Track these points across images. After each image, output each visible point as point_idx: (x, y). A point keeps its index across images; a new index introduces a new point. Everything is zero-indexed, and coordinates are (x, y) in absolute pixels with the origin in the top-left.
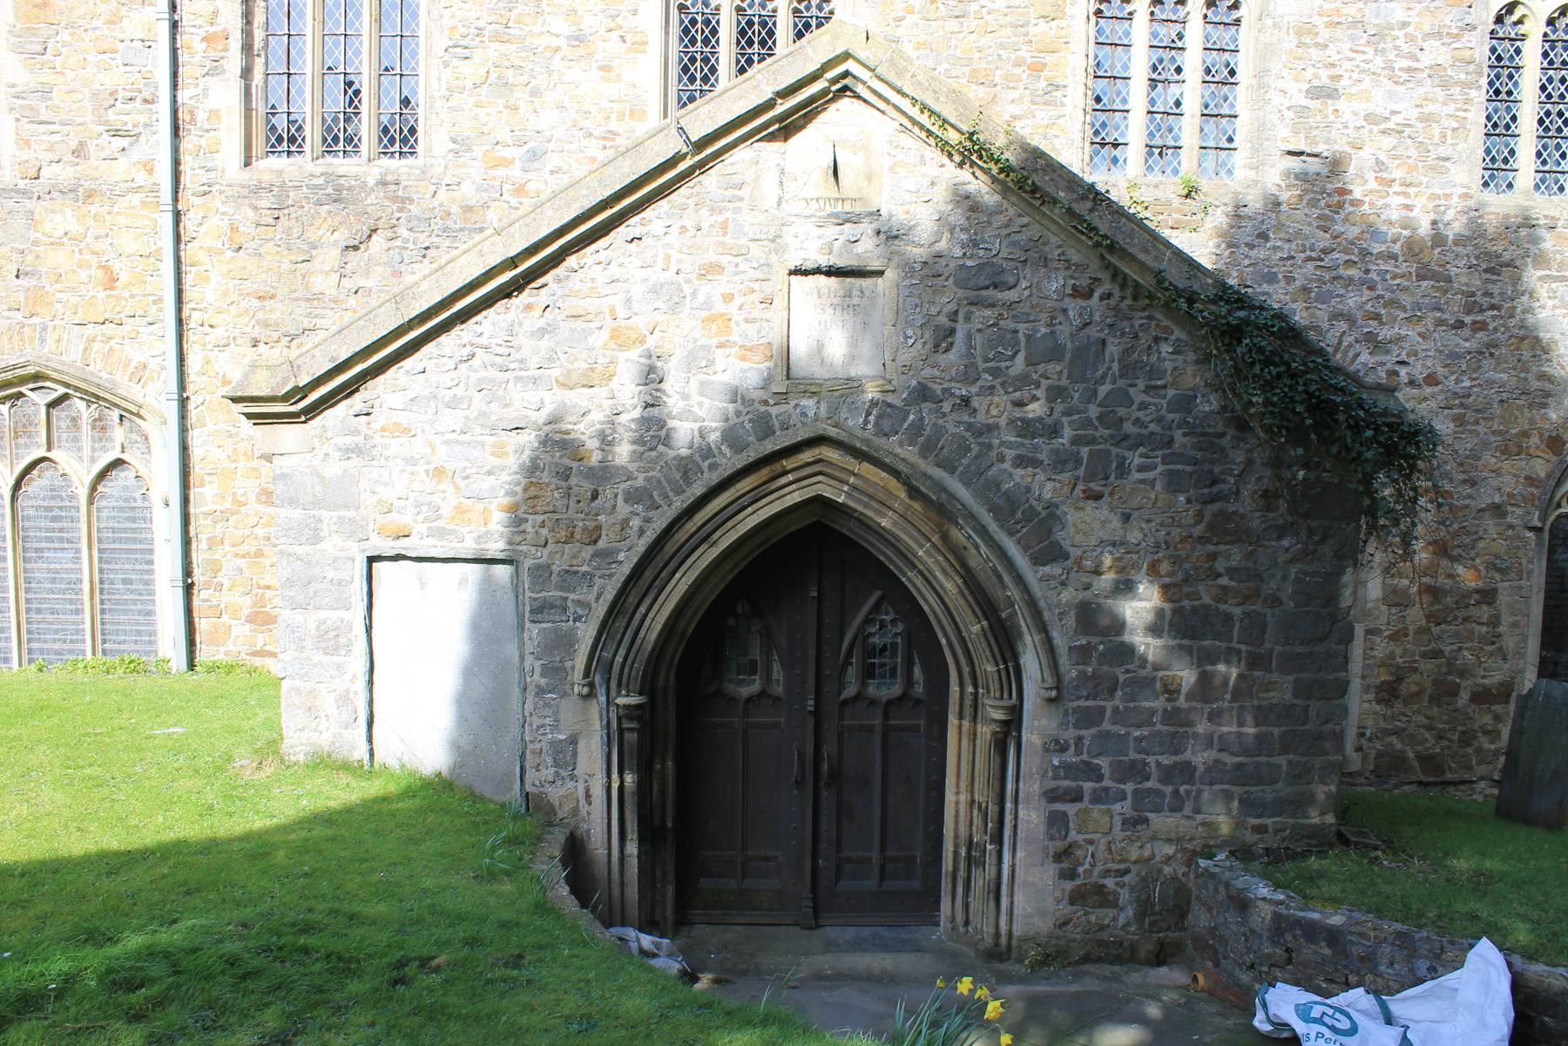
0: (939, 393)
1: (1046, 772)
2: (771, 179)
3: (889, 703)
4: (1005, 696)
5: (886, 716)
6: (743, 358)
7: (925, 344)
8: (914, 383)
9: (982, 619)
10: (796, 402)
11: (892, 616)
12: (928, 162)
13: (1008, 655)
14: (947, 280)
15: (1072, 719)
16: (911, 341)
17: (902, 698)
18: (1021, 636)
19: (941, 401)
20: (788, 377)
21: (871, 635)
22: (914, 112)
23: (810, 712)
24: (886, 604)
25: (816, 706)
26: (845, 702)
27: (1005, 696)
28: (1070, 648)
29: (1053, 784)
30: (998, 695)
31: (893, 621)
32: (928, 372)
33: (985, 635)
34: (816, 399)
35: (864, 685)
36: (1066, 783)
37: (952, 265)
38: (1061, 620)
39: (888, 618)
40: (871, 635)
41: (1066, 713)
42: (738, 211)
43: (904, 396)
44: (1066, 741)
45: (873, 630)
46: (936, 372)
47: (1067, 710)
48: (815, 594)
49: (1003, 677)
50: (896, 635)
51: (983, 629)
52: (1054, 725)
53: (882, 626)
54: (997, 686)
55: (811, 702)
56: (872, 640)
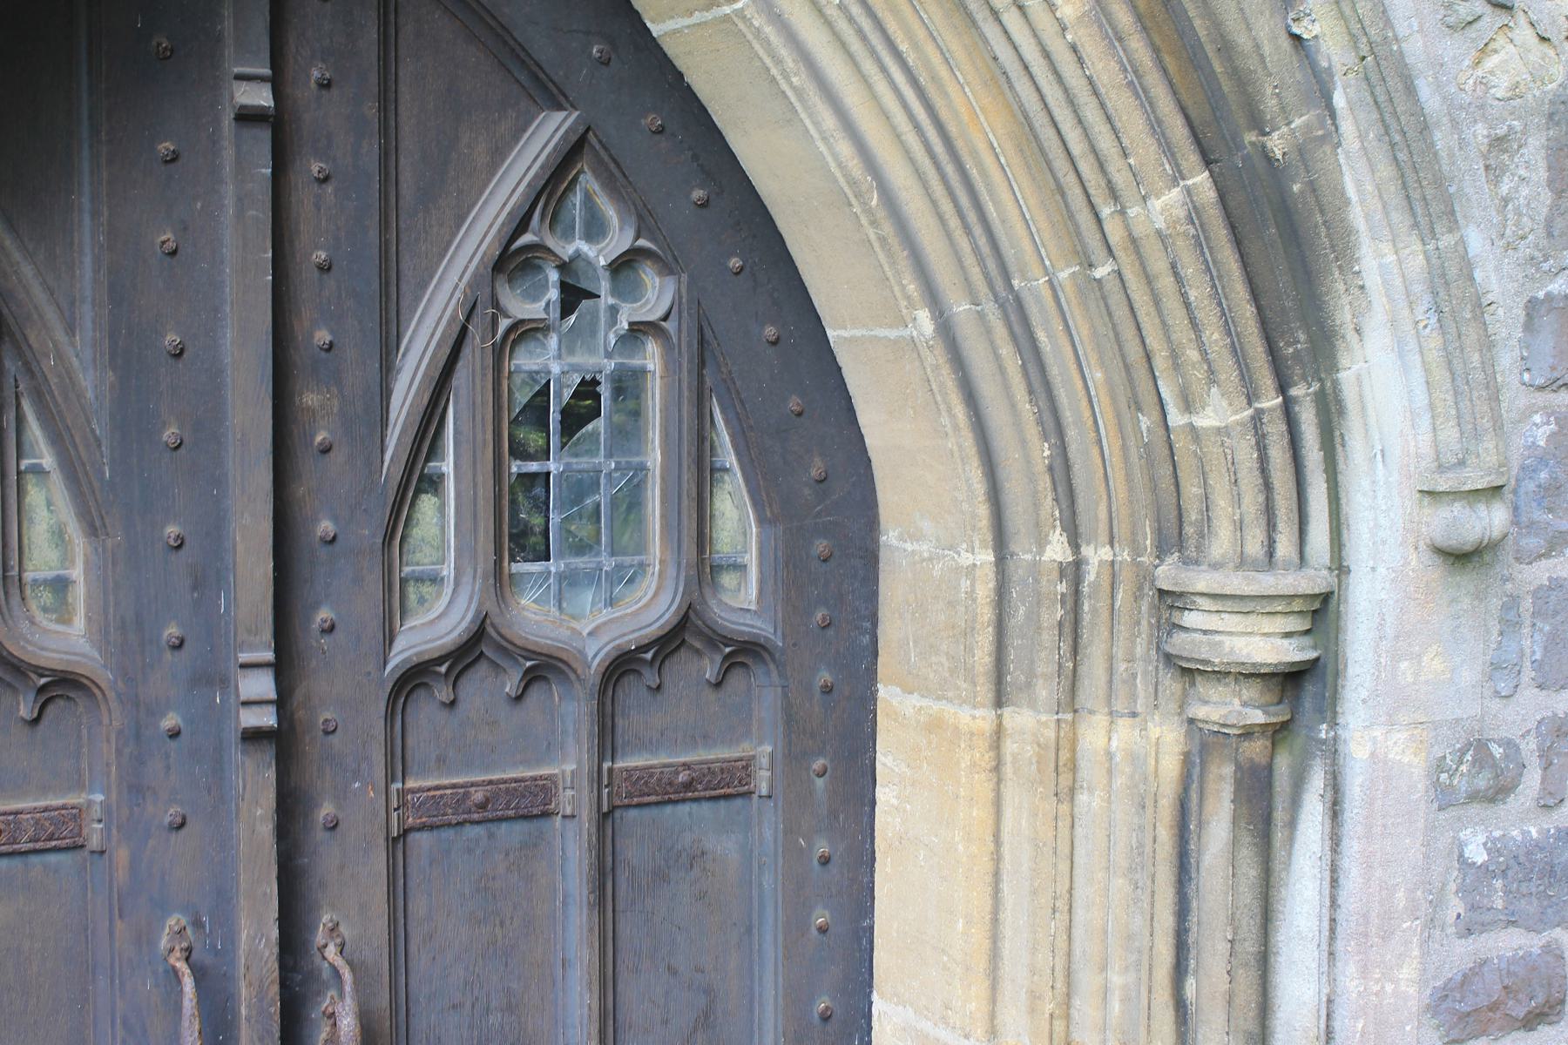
1: (1437, 904)
3: (622, 666)
4: (1285, 546)
5: (606, 739)
9: (1191, 158)
11: (619, 240)
13: (1297, 343)
15: (1531, 644)
17: (670, 642)
18: (1345, 251)
21: (525, 332)
23: (253, 736)
24: (589, 181)
25: (282, 703)
26: (414, 678)
27: (1285, 546)
28: (1532, 306)
29: (1460, 953)
30: (1254, 546)
31: (623, 265)
33: (1201, 243)
35: (500, 583)
36: (1508, 943)
38: (1494, 172)
39: (600, 254)
40: (525, 332)
41: (1510, 624)
44: (1508, 744)
45: (532, 310)
47: (1513, 602)
48: (261, 97)
49: (1278, 455)
50: (639, 330)
51: (1195, 214)
52: (1469, 675)
53: (573, 296)
54: (1252, 501)
55: (261, 685)
56: (526, 360)
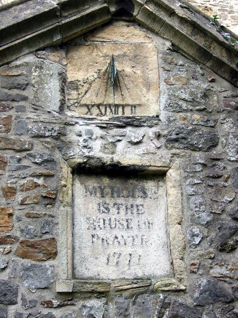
0: (230, 291)
2: (54, 85)
6: (24, 256)
7: (212, 241)
8: (204, 281)
10: (81, 303)
12: (199, 77)
14: (226, 181)
16: (197, 240)
19: (232, 301)
20: (74, 276)
22: (185, 31)
32: (217, 271)
34: (104, 300)
37: (229, 168)
42: (22, 109)
43: (196, 295)
46: (224, 271)
